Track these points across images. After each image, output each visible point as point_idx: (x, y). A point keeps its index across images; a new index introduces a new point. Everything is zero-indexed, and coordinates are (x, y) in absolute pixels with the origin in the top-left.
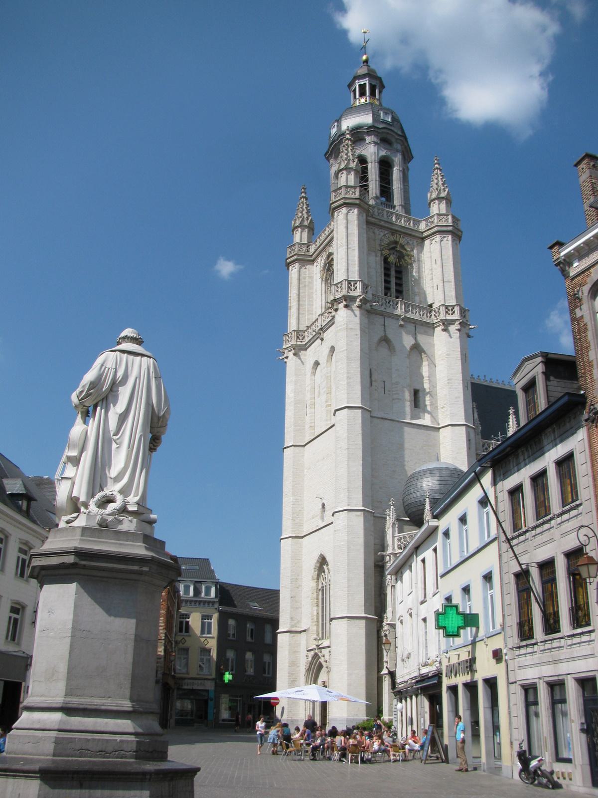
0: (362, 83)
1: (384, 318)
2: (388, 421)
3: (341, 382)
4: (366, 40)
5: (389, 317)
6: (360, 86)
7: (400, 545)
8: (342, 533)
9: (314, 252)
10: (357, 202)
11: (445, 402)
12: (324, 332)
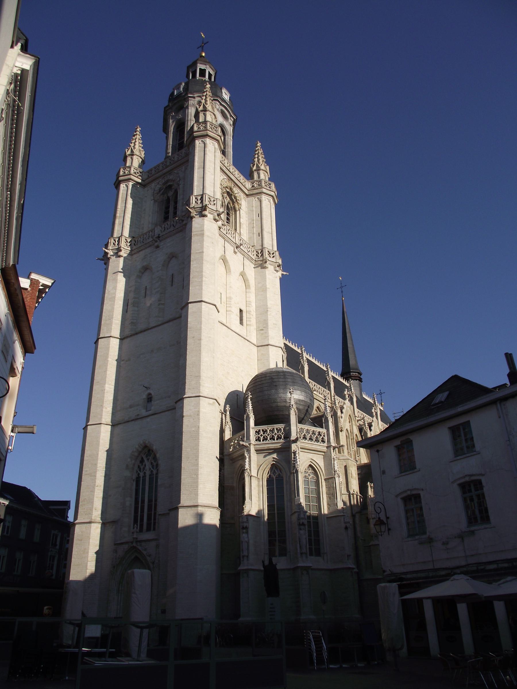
0: (203, 68)
1: (225, 241)
2: (225, 327)
3: (196, 279)
4: (204, 42)
5: (228, 242)
6: (200, 69)
7: (259, 437)
8: (193, 419)
9: (148, 179)
10: (219, 138)
11: (264, 326)
12: (160, 241)
